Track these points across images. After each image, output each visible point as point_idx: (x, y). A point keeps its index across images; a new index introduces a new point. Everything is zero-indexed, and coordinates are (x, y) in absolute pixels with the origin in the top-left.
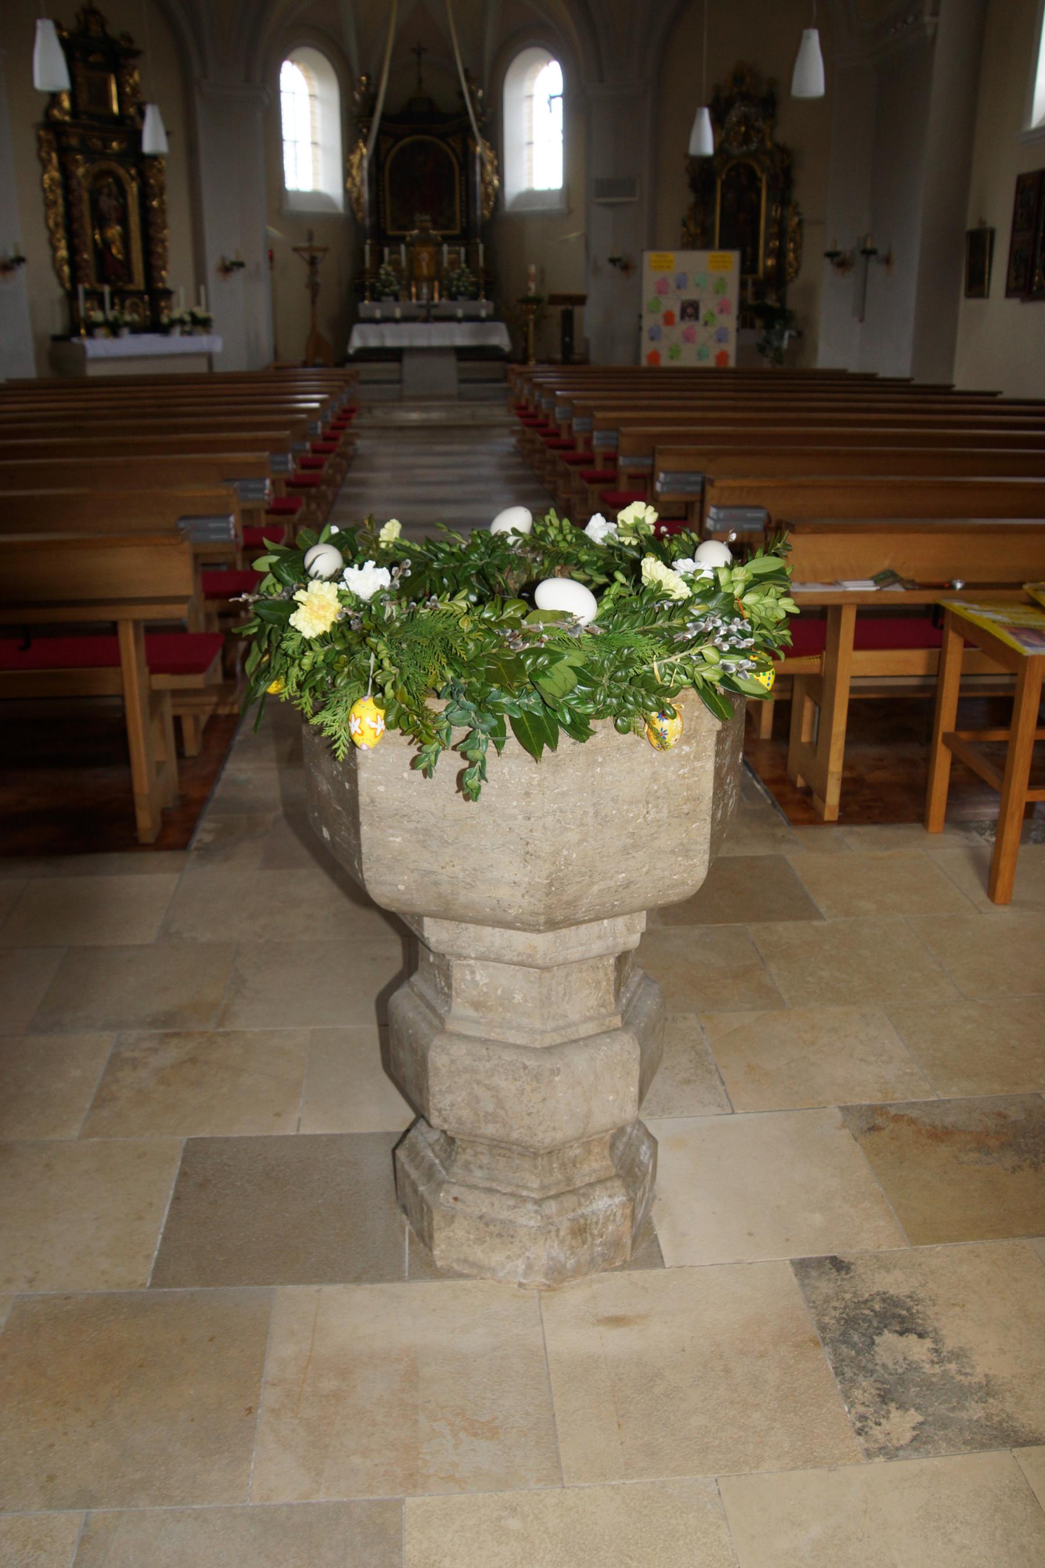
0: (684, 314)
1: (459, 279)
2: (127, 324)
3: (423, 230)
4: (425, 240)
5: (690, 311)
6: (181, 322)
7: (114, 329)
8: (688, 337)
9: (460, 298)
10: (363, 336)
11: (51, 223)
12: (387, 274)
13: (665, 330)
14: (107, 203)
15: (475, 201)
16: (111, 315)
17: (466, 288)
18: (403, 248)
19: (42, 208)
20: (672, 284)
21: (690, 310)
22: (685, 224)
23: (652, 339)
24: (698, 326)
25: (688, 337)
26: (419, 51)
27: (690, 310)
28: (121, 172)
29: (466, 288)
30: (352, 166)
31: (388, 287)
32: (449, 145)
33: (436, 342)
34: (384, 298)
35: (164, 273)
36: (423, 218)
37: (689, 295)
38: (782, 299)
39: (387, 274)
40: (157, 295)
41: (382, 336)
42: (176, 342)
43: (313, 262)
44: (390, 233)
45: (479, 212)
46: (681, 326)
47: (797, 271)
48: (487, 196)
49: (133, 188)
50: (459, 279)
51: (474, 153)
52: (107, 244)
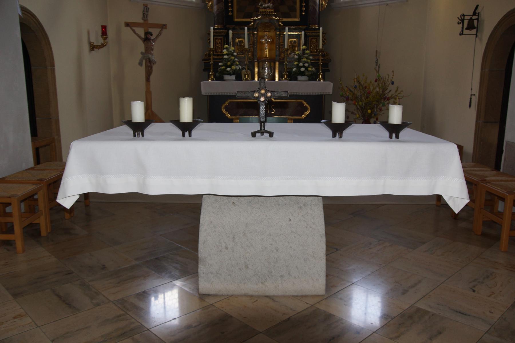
1: (299, 60)
4: (268, 26)
9: (299, 78)
10: (95, 168)
17: (306, 68)
18: (246, 28)
29: (306, 68)
31: (230, 66)
34: (226, 77)
39: (230, 54)
43: (147, 39)
44: (236, 20)
50: (299, 60)
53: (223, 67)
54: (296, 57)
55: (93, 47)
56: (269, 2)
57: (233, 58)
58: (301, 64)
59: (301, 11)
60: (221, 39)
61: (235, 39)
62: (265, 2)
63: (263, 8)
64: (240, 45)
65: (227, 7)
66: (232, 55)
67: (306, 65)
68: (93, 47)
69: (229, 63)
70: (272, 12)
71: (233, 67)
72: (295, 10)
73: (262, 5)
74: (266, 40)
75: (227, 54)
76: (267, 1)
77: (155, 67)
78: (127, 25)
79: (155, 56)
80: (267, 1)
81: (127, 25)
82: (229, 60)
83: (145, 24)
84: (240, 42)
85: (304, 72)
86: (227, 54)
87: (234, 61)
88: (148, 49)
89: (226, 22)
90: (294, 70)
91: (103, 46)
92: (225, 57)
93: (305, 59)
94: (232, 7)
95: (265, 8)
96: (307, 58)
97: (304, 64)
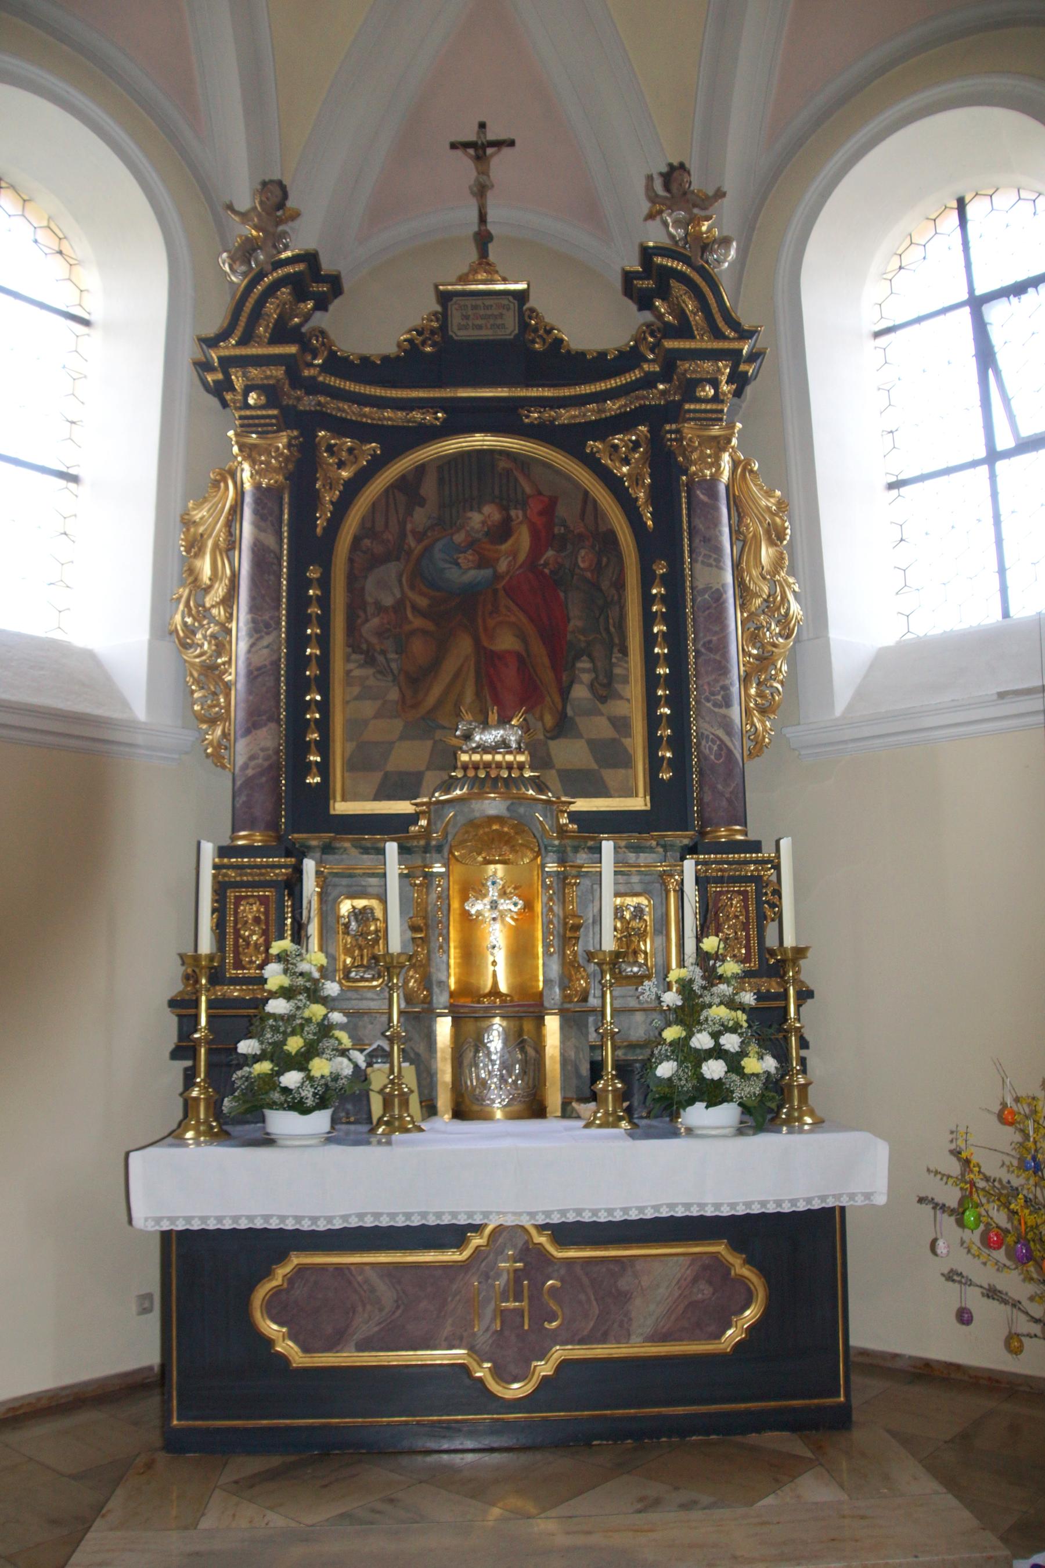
1: (689, 1013)
9: (696, 1115)
18: (392, 848)
26: (480, 149)
29: (734, 1062)
31: (301, 1062)
32: (592, 463)
36: (496, 742)
44: (341, 807)
50: (689, 1013)
51: (711, 485)
53: (264, 1067)
54: (672, 998)
56: (504, 721)
57: (317, 1011)
58: (702, 1041)
59: (654, 764)
60: (264, 901)
61: (336, 903)
62: (486, 726)
63: (474, 750)
64: (363, 934)
66: (314, 994)
67: (731, 1042)
69: (294, 1044)
70: (521, 767)
71: (320, 1067)
72: (627, 762)
73: (468, 737)
74: (494, 905)
75: (287, 993)
76: (493, 717)
80: (493, 717)
82: (290, 1024)
84: (362, 916)
85: (718, 1084)
86: (287, 993)
87: (325, 1029)
90: (665, 1069)
92: (277, 1006)
93: (720, 1012)
94: (324, 747)
95: (484, 749)
96: (731, 1004)
97: (715, 1036)
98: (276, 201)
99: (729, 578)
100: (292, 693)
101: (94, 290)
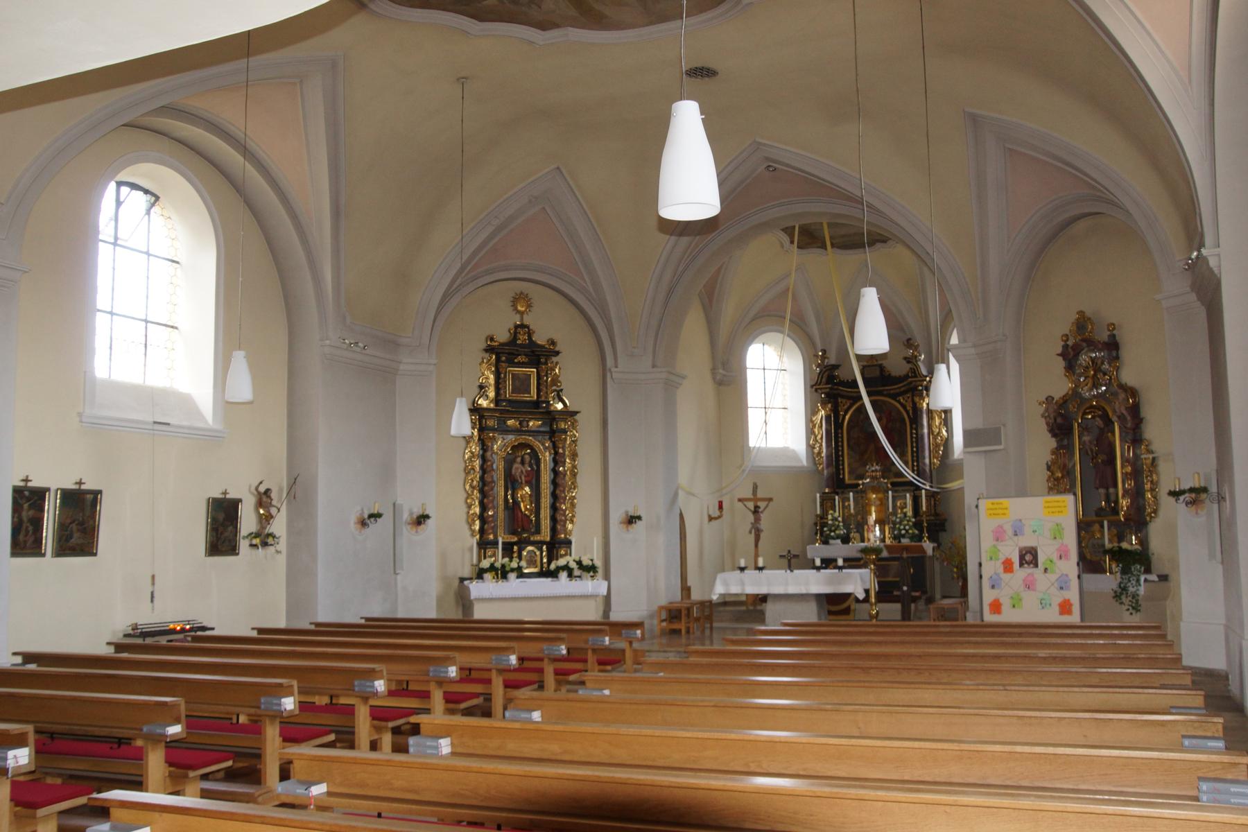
0: (1022, 562)
1: (900, 523)
2: (512, 570)
3: (873, 478)
5: (1028, 557)
6: (566, 568)
7: (503, 574)
8: (1029, 585)
10: (726, 584)
11: (467, 487)
12: (835, 519)
13: (1006, 577)
14: (517, 468)
15: (923, 451)
16: (500, 560)
19: (463, 475)
20: (1010, 532)
21: (1029, 557)
22: (1049, 468)
23: (993, 587)
24: (1038, 573)
25: (1029, 585)
27: (1029, 557)
28: (538, 446)
30: (814, 426)
32: (899, 402)
33: (792, 590)
34: (831, 541)
35: (570, 526)
37: (1027, 541)
38: (1143, 542)
39: (835, 519)
40: (557, 545)
41: (743, 584)
42: (563, 584)
43: (756, 511)
45: (927, 461)
46: (1021, 573)
47: (1155, 512)
48: (937, 446)
49: (547, 458)
50: (900, 523)
52: (516, 504)
55: (711, 519)
65: (838, 469)
68: (711, 519)
77: (762, 535)
78: (740, 500)
79: (763, 524)
81: (740, 500)
83: (755, 499)
88: (757, 520)
89: (837, 485)
91: (719, 517)
98: (824, 357)
99: (926, 431)
100: (835, 460)
101: (787, 363)
